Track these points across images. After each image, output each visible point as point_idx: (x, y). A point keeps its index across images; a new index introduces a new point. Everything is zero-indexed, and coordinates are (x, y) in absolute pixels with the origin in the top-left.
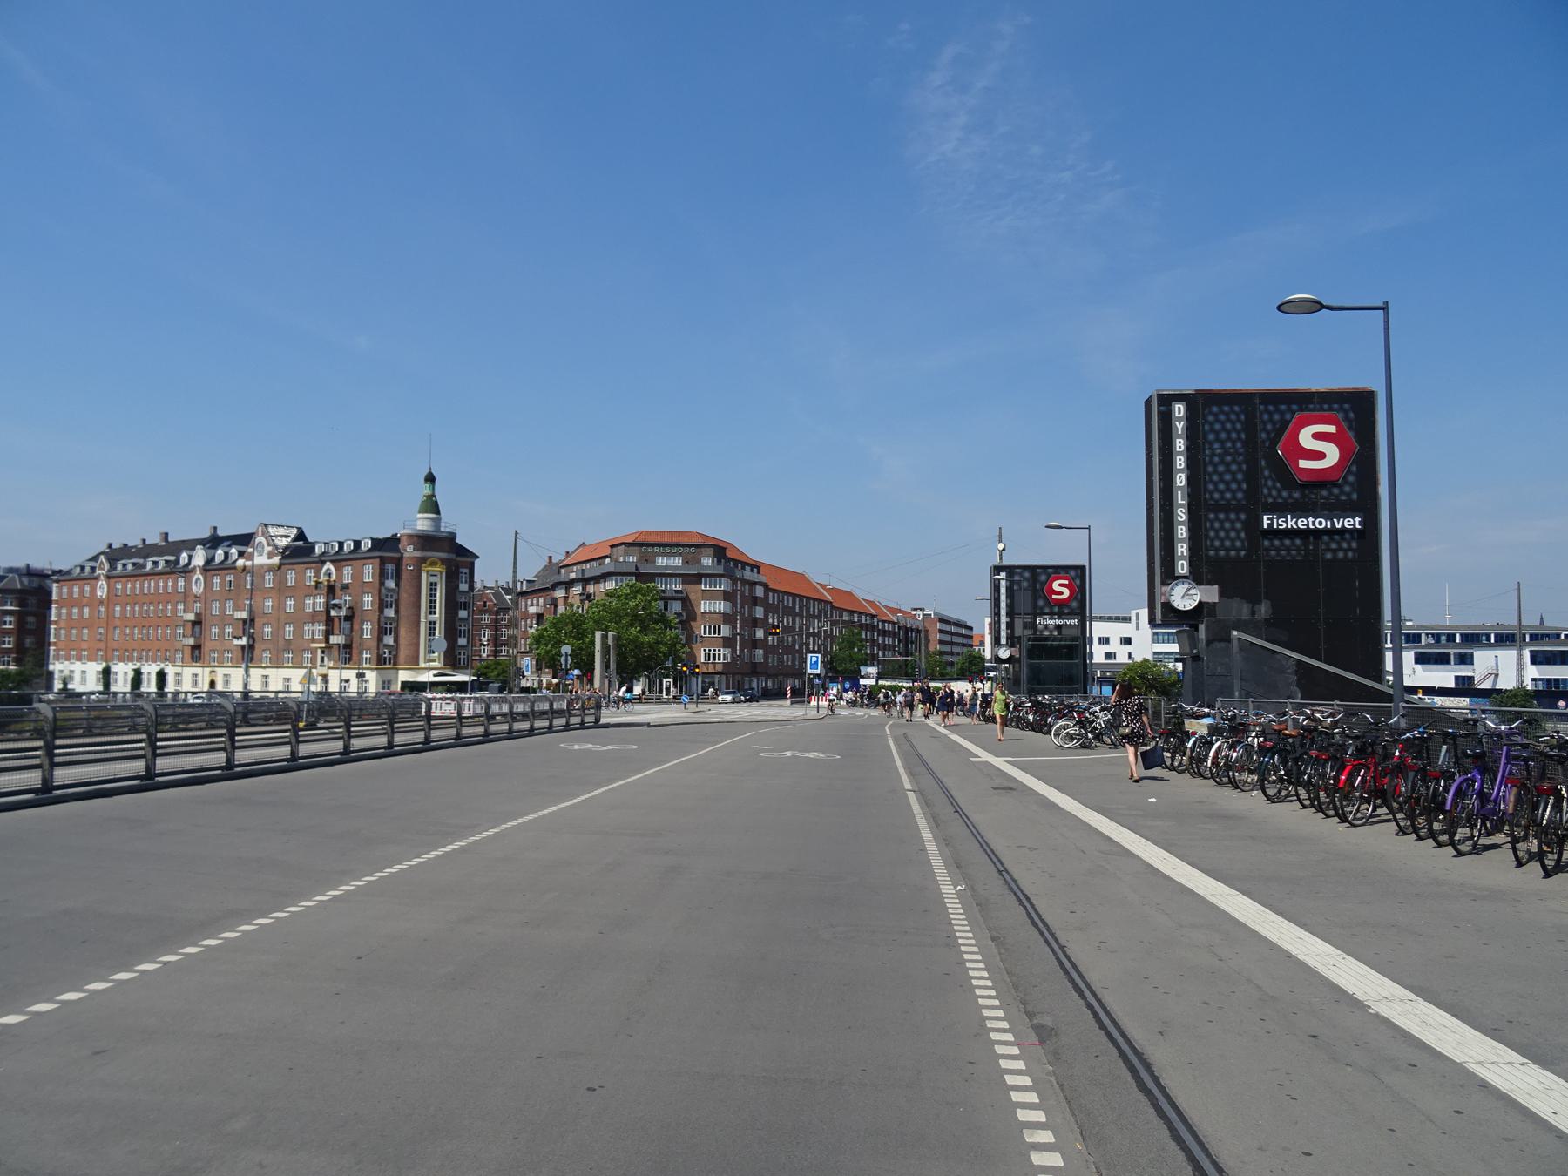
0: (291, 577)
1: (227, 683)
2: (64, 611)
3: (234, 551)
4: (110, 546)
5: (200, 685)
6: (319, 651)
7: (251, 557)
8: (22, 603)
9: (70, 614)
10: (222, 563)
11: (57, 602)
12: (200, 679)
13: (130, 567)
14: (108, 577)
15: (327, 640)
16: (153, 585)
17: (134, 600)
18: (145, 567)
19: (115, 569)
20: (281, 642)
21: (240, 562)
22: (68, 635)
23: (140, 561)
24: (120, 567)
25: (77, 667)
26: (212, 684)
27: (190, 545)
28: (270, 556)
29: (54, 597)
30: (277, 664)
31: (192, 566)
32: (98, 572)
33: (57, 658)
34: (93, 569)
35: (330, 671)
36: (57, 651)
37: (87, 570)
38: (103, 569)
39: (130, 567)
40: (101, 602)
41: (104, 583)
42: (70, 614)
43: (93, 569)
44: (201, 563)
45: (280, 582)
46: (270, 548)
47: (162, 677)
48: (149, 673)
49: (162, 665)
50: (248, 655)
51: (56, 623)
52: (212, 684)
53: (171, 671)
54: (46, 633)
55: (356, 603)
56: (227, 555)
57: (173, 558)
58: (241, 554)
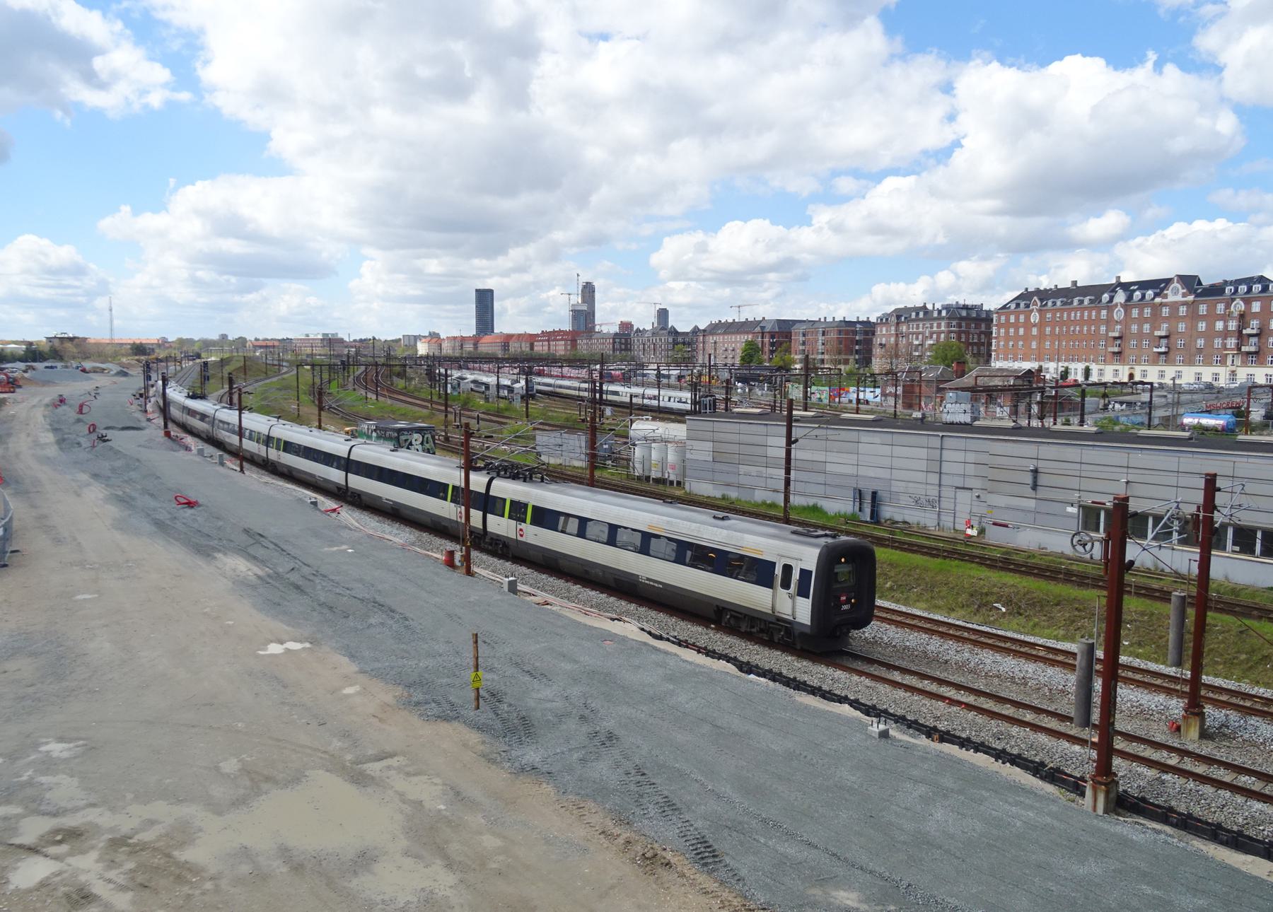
0: (1203, 309)
1: (1145, 376)
2: (1002, 331)
3: (1150, 293)
4: (1027, 289)
5: (1120, 376)
6: (1231, 356)
7: (1166, 296)
8: (960, 326)
9: (1007, 332)
10: (1141, 300)
11: (996, 326)
12: (1120, 373)
13: (1059, 303)
14: (1039, 311)
15: (1239, 349)
16: (1078, 315)
17: (1062, 323)
18: (1072, 303)
19: (1046, 304)
20: (1194, 350)
21: (1158, 300)
22: (1006, 345)
23: (1065, 300)
24: (1050, 303)
25: (1072, 366)
26: (1131, 376)
27: (1112, 289)
28: (1184, 295)
29: (995, 322)
30: (1189, 362)
31: (1114, 302)
32: (1031, 307)
33: (997, 359)
34: (1027, 306)
35: (1239, 368)
36: (998, 355)
37: (1022, 305)
38: (1037, 305)
39: (1059, 303)
40: (1035, 325)
41: (1037, 314)
42: (1007, 332)
43: (1027, 306)
44: (1123, 301)
45: (1193, 312)
46: (1185, 291)
47: (1087, 372)
48: (1076, 369)
49: (1087, 364)
50: (1166, 357)
51: (996, 338)
52: (1131, 376)
53: (1094, 368)
54: (990, 344)
55: (1264, 325)
56: (1143, 296)
57: (1093, 298)
58: (1156, 295)
